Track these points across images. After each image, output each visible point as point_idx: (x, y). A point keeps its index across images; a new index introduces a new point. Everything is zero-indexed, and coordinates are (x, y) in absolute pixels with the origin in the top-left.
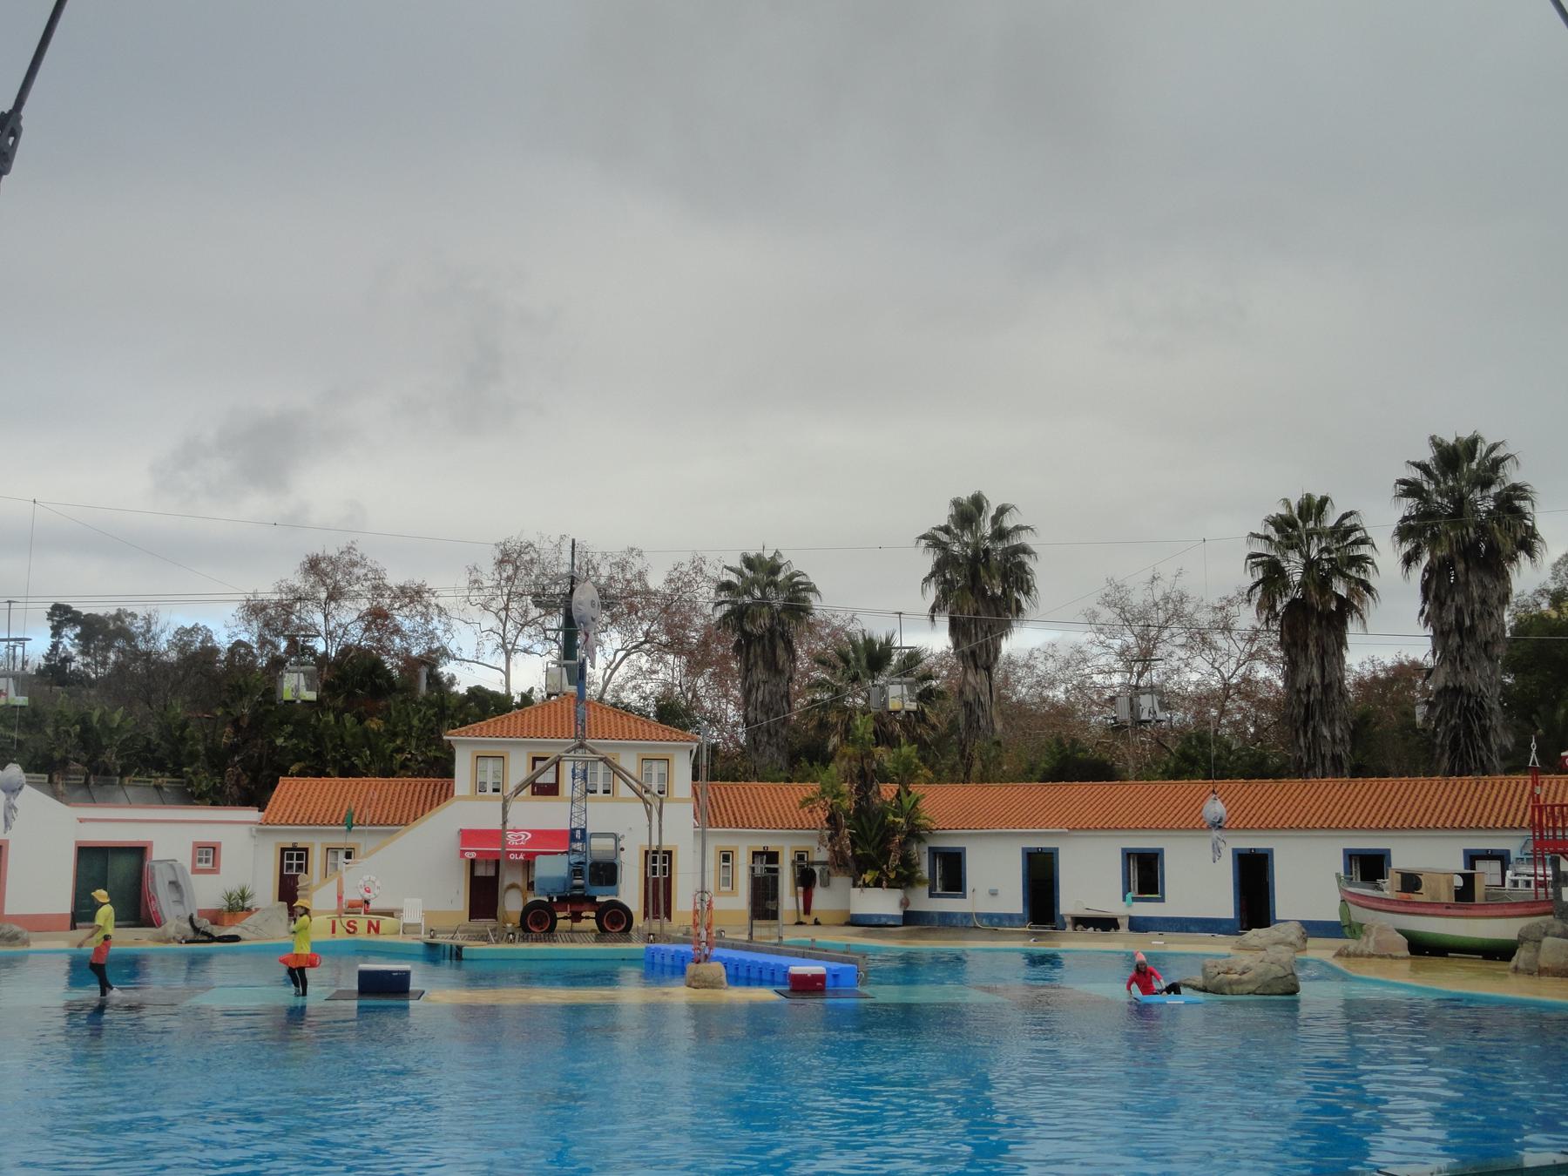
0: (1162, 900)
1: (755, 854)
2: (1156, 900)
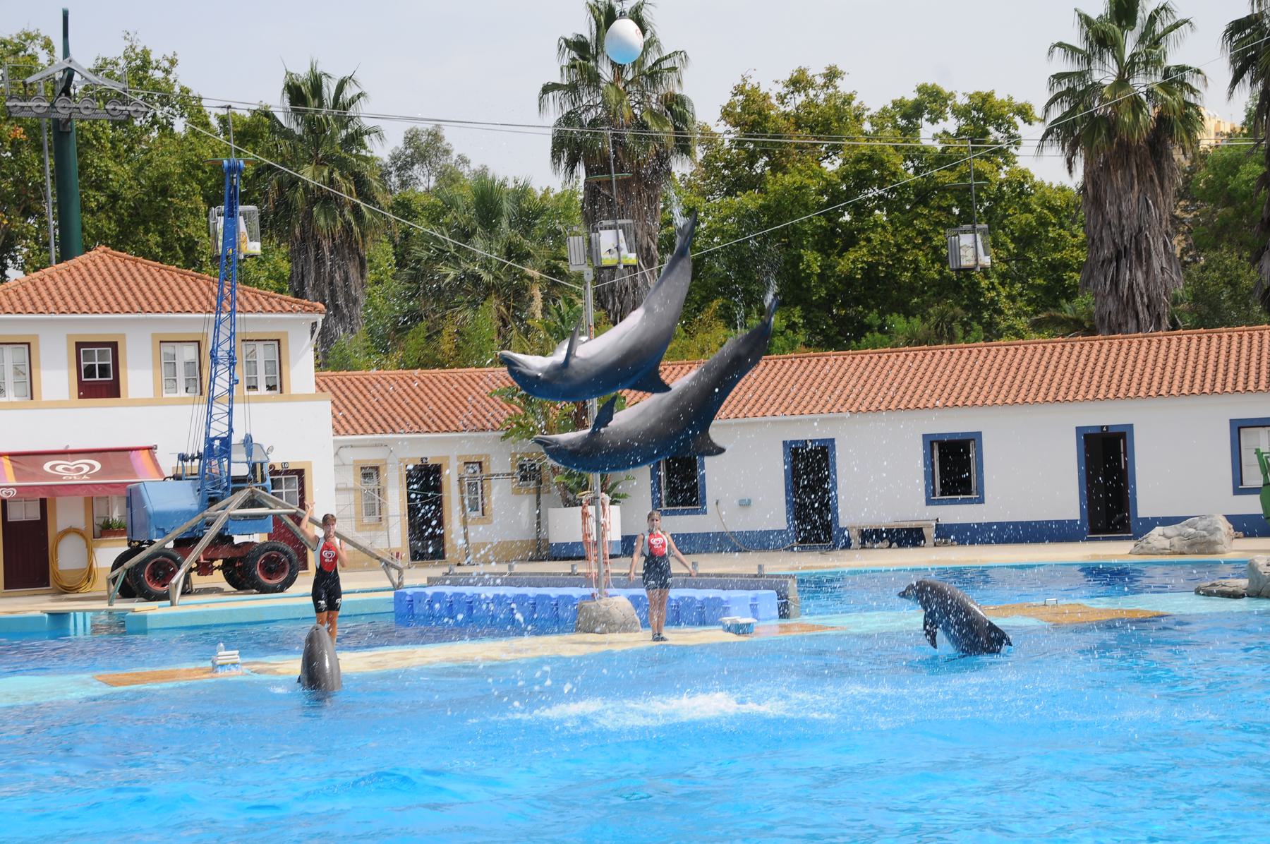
0: (981, 501)
2: (971, 501)
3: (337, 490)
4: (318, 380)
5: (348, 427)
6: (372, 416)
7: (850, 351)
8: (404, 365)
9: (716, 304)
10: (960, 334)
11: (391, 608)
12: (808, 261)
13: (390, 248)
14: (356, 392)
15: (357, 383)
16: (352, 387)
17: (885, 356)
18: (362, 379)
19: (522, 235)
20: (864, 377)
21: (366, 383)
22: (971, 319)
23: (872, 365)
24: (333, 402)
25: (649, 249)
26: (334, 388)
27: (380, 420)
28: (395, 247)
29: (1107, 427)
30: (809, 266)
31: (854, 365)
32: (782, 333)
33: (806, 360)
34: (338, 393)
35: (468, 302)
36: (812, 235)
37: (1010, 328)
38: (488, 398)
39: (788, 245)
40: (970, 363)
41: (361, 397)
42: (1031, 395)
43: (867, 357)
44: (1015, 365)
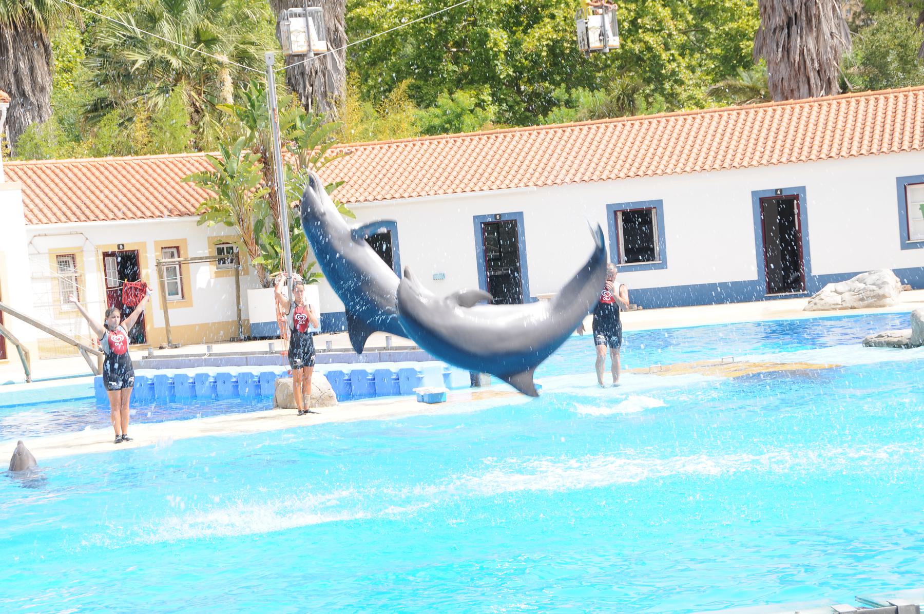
0: (663, 265)
1: (105, 255)
3: (33, 278)
4: (8, 170)
5: (40, 216)
6: (65, 204)
7: (535, 127)
8: (98, 154)
9: (404, 84)
10: (644, 105)
11: (92, 393)
12: (495, 40)
13: (77, 35)
14: (48, 181)
15: (48, 172)
16: (43, 176)
17: (569, 130)
18: (53, 168)
19: (208, 18)
20: (549, 151)
21: (57, 171)
22: (654, 90)
23: (556, 139)
24: (23, 191)
25: (336, 30)
26: (24, 177)
27: (74, 208)
28: (83, 33)
29: (781, 190)
30: (496, 44)
31: (539, 140)
32: (472, 111)
33: (493, 137)
34: (29, 182)
35: (159, 88)
36: (498, 13)
37: (690, 98)
38: (183, 184)
39: (474, 23)
40: (650, 133)
41: (52, 185)
42: (709, 162)
43: (552, 132)
44: (693, 134)
